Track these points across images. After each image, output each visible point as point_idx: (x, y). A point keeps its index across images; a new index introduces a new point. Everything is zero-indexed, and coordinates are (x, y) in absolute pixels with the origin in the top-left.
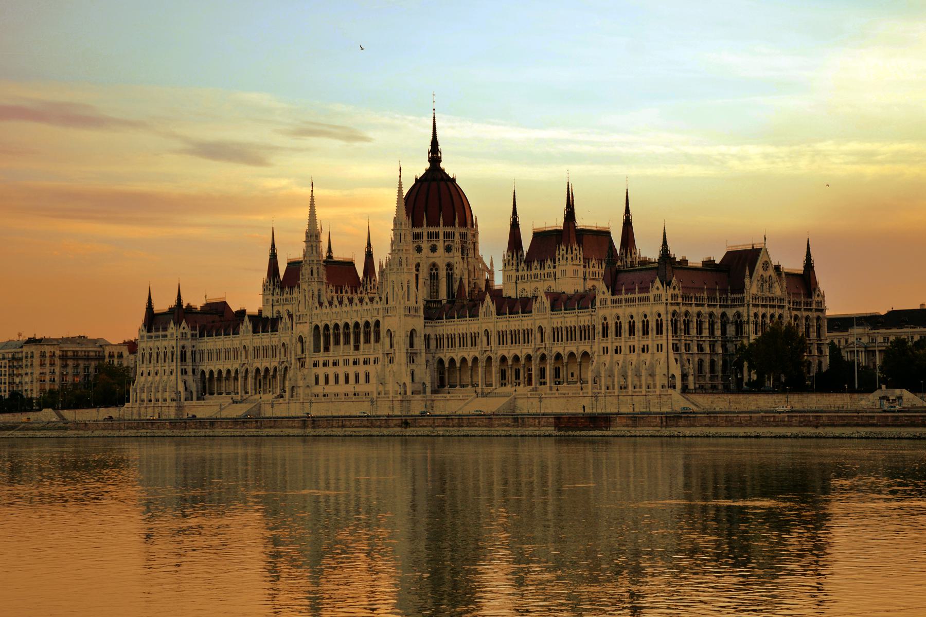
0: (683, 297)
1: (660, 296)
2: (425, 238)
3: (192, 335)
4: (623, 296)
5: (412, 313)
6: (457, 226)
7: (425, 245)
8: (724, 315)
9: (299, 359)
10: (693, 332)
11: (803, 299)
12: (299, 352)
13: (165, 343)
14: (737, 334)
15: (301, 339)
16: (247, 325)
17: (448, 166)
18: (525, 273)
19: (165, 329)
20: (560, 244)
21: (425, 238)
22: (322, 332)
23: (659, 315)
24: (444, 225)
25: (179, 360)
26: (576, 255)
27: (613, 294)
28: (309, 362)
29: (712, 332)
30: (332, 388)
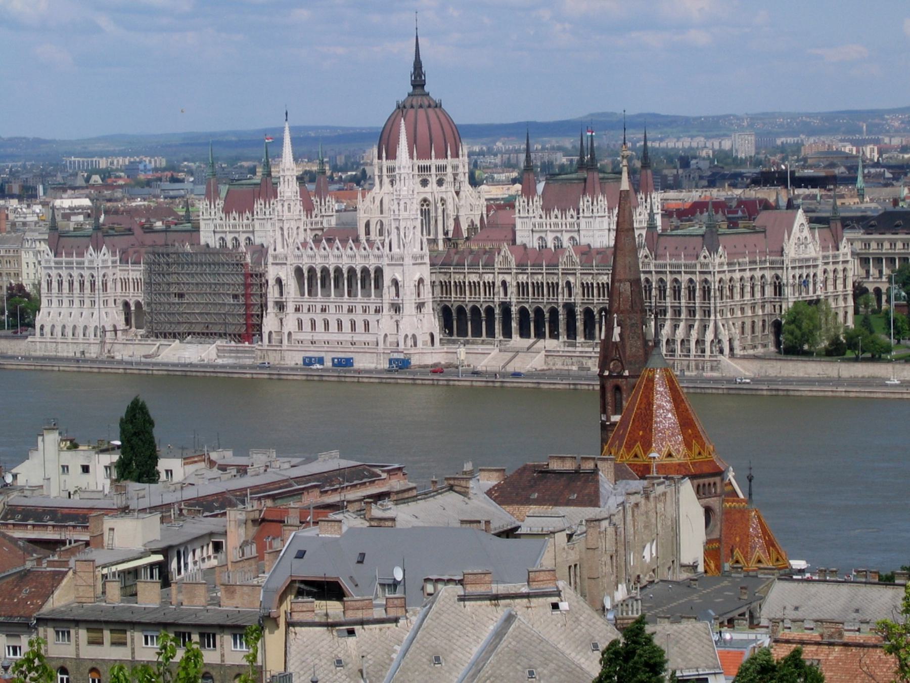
0: (729, 264)
3: (114, 262)
6: (449, 158)
7: (418, 180)
8: (763, 277)
10: (737, 297)
11: (831, 253)
12: (277, 295)
14: (775, 294)
15: (279, 281)
18: (544, 220)
19: (81, 254)
20: (584, 194)
22: (306, 275)
24: (436, 157)
25: (101, 291)
28: (290, 308)
29: (753, 295)
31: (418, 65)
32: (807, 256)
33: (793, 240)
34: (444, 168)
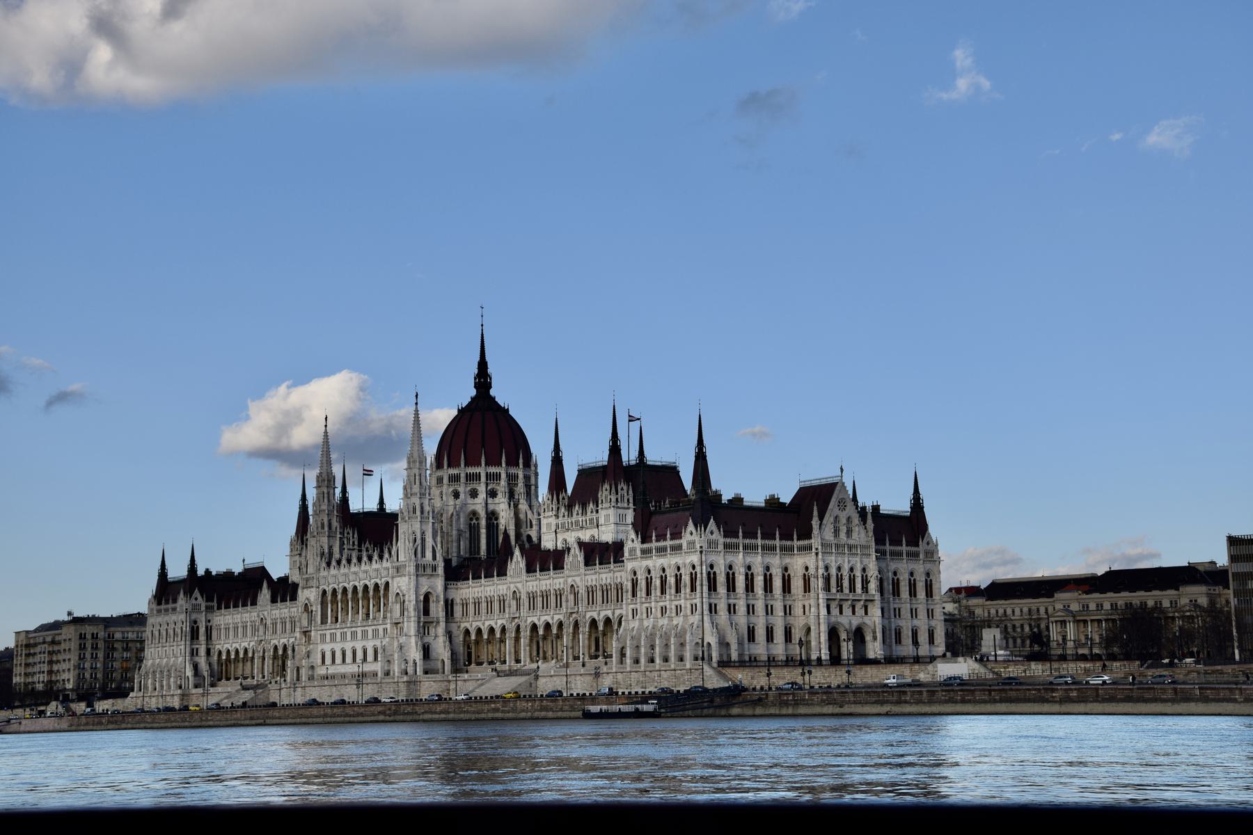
1: (694, 543)
2: (463, 480)
4: (654, 545)
5: (429, 571)
9: (305, 632)
12: (305, 623)
13: (174, 617)
16: (265, 594)
17: (499, 393)
19: (175, 601)
21: (463, 480)
23: (694, 567)
24: (486, 464)
25: (188, 638)
26: (622, 497)
27: (643, 542)
30: (339, 669)
31: (483, 365)
32: (851, 542)
33: (828, 518)
34: (497, 477)
